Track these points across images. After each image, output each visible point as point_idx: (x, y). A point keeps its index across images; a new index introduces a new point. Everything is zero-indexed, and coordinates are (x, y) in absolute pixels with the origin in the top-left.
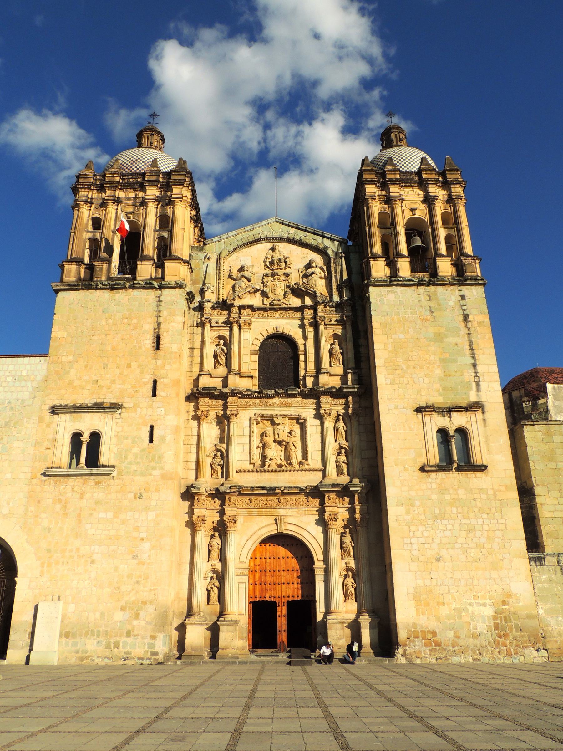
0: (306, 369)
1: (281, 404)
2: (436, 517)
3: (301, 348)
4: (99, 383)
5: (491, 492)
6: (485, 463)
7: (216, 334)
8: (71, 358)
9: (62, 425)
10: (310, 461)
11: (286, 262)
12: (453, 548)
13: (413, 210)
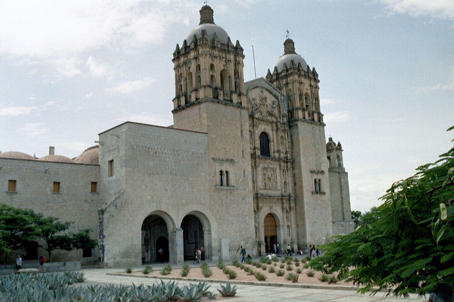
2: (315, 209)
3: (272, 139)
6: (325, 192)
9: (217, 166)
10: (278, 187)
11: (266, 100)
13: (307, 89)
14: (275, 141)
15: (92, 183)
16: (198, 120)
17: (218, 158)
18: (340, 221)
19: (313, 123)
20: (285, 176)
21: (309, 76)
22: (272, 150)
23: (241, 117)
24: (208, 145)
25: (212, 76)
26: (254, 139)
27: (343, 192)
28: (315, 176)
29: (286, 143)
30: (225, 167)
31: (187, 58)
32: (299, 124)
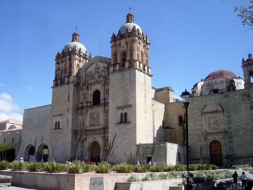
1: (95, 109)
5: (130, 129)
7: (83, 92)
12: (121, 144)
20: (107, 115)
24: (51, 110)
28: (121, 111)
30: (59, 119)
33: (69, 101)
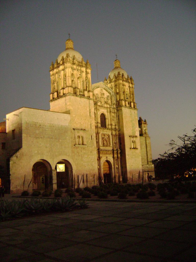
0: (108, 122)
2: (132, 158)
3: (107, 118)
4: (81, 123)
8: (75, 115)
9: (76, 133)
13: (127, 89)
14: (109, 119)
15: (2, 143)
16: (65, 106)
17: (76, 129)
18: (146, 165)
19: (131, 108)
21: (128, 81)
22: (107, 123)
23: (89, 105)
24: (70, 121)
25: (73, 81)
26: (97, 117)
27: (148, 148)
28: (132, 139)
29: (115, 120)
30: (81, 133)
31: (58, 70)
32: (123, 109)
33: (91, 118)
